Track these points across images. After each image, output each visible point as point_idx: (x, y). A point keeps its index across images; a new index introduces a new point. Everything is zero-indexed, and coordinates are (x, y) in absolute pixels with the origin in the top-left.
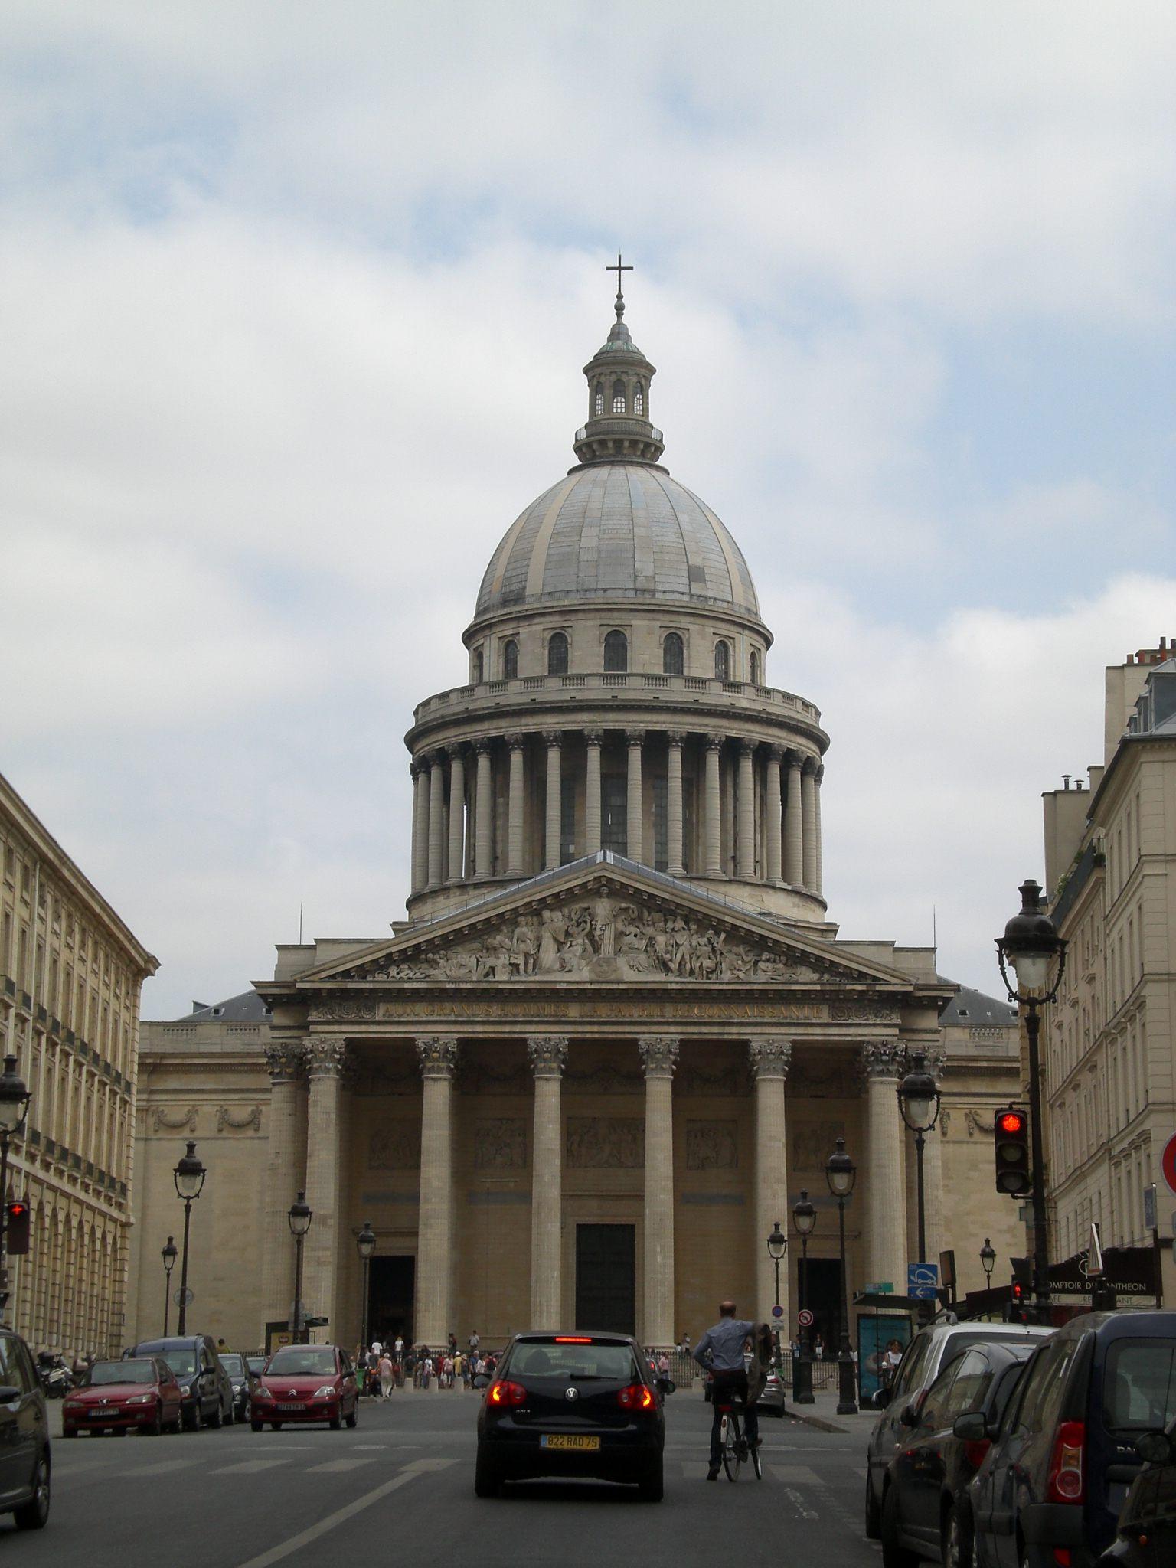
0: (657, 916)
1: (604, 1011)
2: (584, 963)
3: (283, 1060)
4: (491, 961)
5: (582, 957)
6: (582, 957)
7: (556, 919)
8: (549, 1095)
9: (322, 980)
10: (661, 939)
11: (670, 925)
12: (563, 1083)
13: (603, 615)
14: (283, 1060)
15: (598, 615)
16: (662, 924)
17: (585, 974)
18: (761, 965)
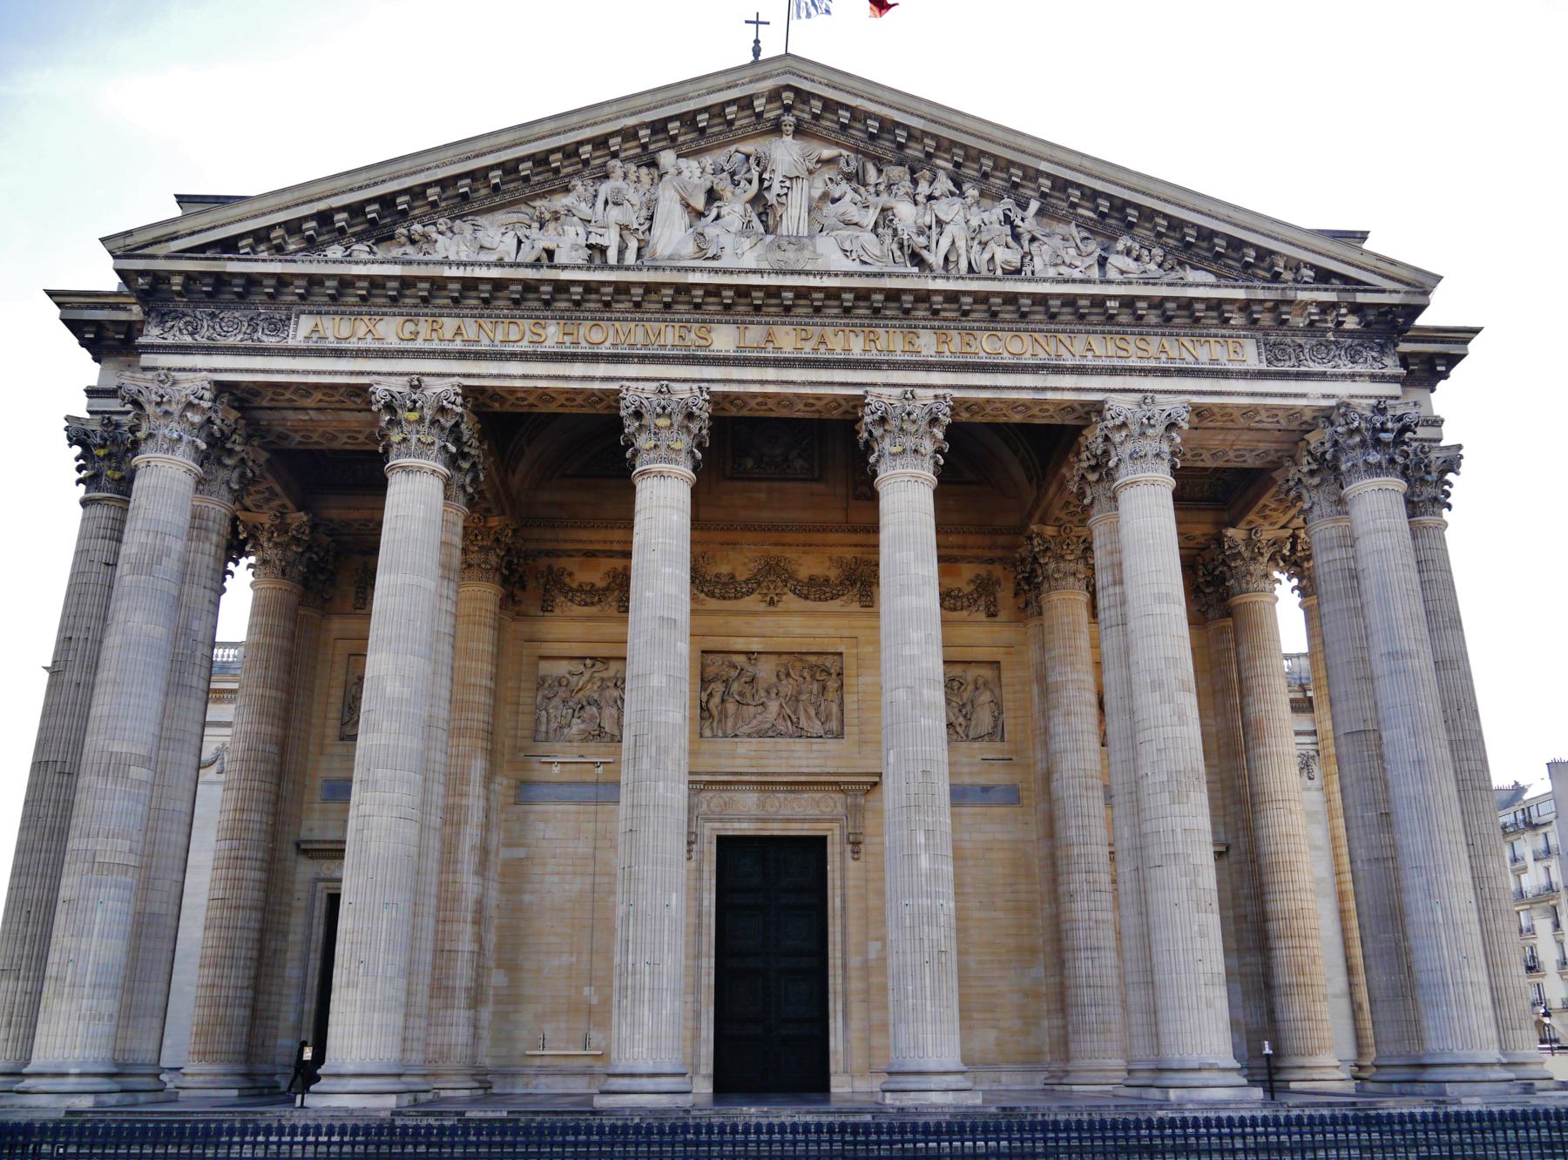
0: (896, 172)
1: (787, 340)
3: (101, 452)
4: (544, 240)
5: (741, 233)
6: (741, 233)
7: (689, 173)
8: (663, 503)
10: (906, 214)
11: (924, 188)
12: (695, 492)
14: (101, 452)
16: (906, 184)
18: (1116, 261)
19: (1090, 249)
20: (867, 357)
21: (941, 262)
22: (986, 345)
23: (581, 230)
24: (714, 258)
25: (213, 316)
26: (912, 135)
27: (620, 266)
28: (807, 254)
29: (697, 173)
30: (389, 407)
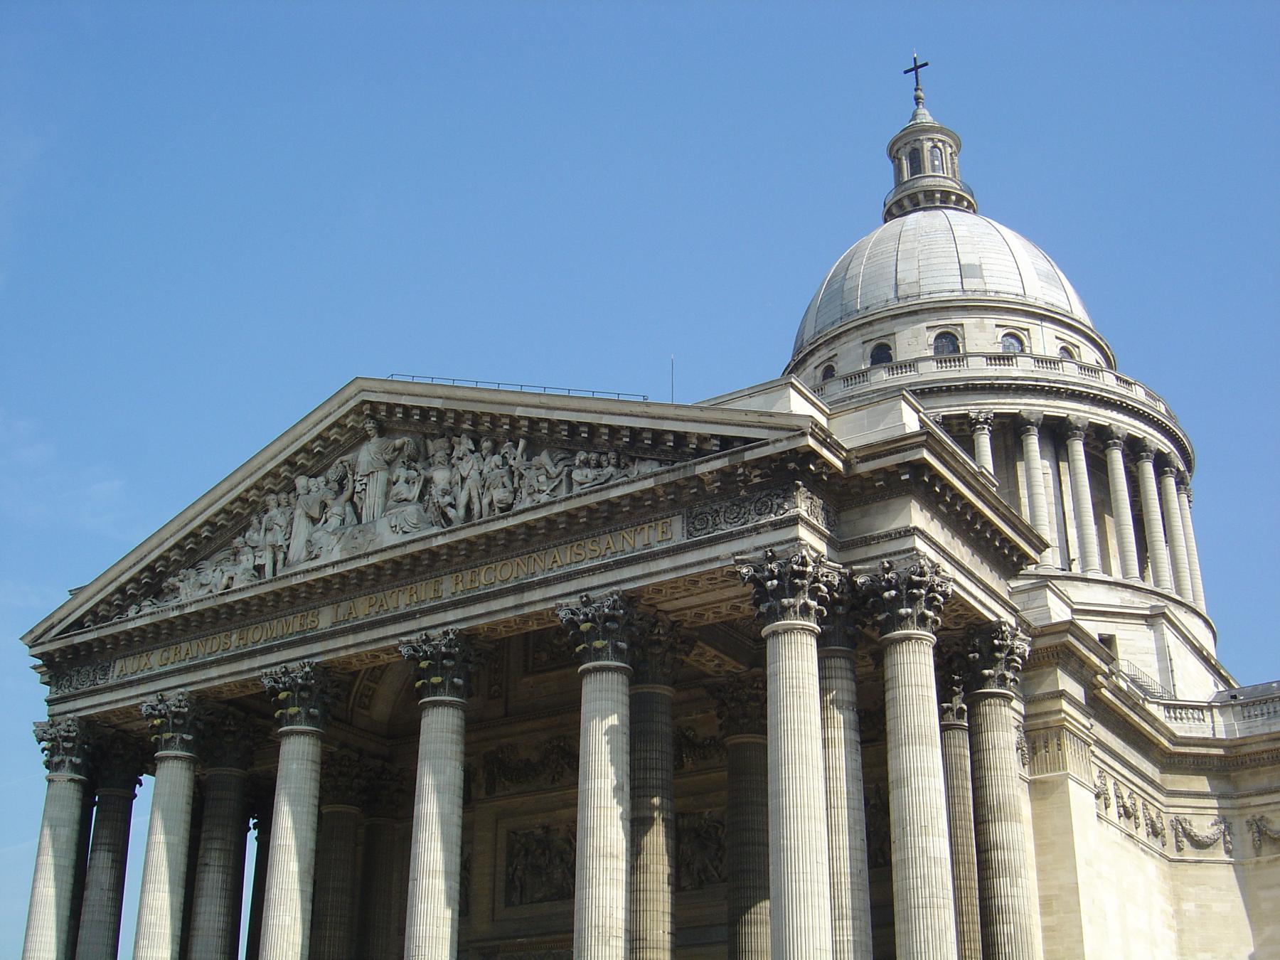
1: (363, 608)
2: (335, 539)
4: (229, 570)
5: (334, 533)
6: (334, 533)
9: (50, 641)
10: (441, 476)
13: (864, 331)
15: (859, 333)
17: (336, 556)
18: (577, 475)
19: (557, 471)
20: (408, 609)
21: (462, 512)
22: (485, 578)
23: (251, 556)
24: (317, 557)
25: (78, 672)
26: (441, 413)
27: (276, 578)
28: (369, 536)
29: (322, 485)
30: (151, 716)
